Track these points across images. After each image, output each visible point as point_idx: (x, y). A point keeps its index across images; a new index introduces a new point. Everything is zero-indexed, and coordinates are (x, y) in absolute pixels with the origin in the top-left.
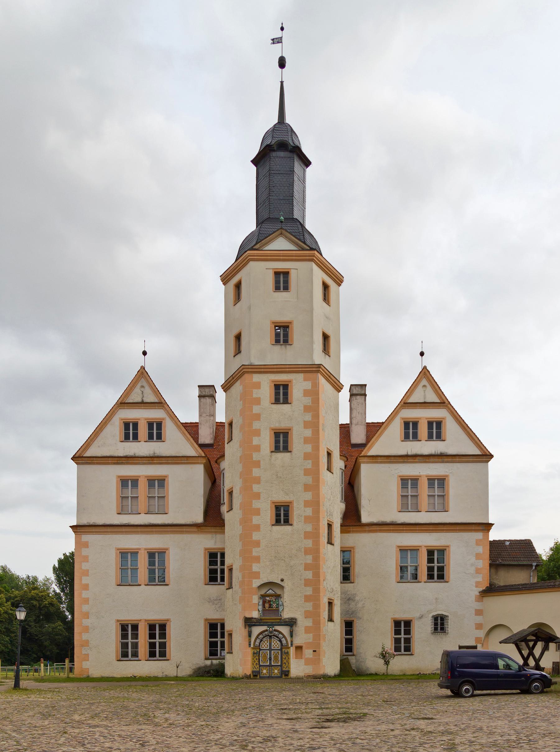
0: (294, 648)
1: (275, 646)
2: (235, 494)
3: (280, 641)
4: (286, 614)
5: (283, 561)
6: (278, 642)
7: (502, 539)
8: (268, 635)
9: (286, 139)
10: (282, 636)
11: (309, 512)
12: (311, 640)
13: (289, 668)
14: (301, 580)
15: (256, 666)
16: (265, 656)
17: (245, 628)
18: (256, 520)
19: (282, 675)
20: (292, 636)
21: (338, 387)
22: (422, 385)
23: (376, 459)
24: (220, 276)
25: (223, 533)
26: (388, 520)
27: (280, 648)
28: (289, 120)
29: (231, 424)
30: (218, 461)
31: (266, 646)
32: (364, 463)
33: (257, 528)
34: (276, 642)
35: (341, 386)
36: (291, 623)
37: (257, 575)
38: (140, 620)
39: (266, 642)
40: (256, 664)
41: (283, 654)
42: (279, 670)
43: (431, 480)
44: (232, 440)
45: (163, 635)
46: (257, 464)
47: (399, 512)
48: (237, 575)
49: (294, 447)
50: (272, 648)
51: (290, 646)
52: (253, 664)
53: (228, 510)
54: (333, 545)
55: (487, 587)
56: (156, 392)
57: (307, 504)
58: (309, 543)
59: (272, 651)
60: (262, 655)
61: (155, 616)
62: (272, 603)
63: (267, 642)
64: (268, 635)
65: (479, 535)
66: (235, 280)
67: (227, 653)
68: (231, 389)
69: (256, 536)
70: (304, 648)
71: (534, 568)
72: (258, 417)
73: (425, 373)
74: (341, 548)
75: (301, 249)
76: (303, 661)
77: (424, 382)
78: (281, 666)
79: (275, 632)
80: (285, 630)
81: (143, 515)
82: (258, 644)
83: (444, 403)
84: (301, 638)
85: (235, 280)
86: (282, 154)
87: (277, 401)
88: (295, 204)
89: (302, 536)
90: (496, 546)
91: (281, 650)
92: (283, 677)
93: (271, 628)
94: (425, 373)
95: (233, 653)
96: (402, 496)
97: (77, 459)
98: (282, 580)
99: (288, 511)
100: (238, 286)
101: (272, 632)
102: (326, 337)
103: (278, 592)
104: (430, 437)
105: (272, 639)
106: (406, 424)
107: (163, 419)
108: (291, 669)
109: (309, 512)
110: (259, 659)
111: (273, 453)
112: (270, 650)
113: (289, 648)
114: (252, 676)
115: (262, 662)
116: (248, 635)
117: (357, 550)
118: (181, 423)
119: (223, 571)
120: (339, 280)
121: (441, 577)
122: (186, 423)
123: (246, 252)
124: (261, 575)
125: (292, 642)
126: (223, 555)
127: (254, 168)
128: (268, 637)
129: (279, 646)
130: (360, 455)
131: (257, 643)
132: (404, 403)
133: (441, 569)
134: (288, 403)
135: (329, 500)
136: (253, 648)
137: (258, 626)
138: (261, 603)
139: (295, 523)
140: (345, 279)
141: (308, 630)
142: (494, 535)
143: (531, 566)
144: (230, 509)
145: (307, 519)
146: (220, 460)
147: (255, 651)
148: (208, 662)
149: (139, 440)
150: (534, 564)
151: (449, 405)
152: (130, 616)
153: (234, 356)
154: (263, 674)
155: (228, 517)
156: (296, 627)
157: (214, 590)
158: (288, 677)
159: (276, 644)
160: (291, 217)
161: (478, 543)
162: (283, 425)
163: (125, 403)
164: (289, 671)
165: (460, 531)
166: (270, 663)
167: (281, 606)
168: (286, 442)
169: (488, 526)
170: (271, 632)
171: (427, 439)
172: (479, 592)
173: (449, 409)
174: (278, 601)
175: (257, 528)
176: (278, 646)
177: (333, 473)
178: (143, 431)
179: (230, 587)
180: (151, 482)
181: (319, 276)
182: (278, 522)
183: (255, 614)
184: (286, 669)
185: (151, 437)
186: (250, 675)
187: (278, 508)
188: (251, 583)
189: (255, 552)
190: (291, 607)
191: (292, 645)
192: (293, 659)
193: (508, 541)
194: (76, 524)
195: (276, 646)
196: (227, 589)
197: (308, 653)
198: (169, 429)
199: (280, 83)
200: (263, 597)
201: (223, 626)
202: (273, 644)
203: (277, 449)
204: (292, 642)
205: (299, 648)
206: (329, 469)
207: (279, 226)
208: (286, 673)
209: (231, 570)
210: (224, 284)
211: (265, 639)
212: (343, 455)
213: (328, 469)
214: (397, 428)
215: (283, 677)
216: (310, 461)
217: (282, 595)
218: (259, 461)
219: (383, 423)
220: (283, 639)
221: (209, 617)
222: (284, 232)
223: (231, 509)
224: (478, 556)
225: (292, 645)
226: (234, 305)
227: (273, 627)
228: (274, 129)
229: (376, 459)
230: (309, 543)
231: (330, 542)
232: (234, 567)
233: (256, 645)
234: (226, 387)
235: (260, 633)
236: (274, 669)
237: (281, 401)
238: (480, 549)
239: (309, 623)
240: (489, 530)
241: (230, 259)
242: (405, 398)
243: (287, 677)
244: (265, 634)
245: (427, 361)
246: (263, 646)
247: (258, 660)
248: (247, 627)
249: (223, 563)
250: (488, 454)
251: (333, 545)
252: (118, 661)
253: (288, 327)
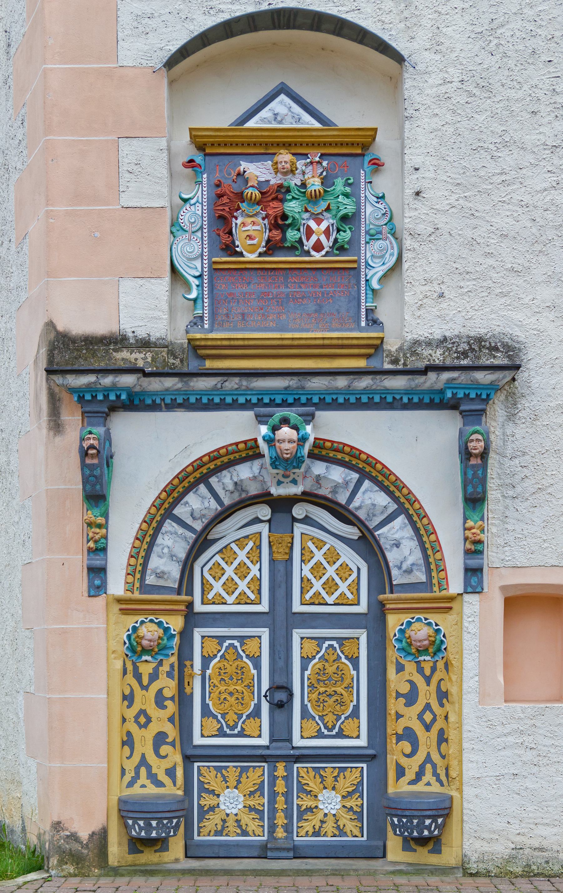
10: (382, 499)
27: (363, 608)
31: (242, 586)
42: (357, 789)
59: (297, 634)
79: (319, 468)
82: (175, 571)
108: (468, 791)
115: (212, 725)
128: (264, 512)
137: (172, 406)
156: (511, 417)
158: (434, 860)
176: (343, 587)
190: (472, 243)
192: (483, 697)
233: (150, 580)
235: (182, 476)
236: (313, 785)
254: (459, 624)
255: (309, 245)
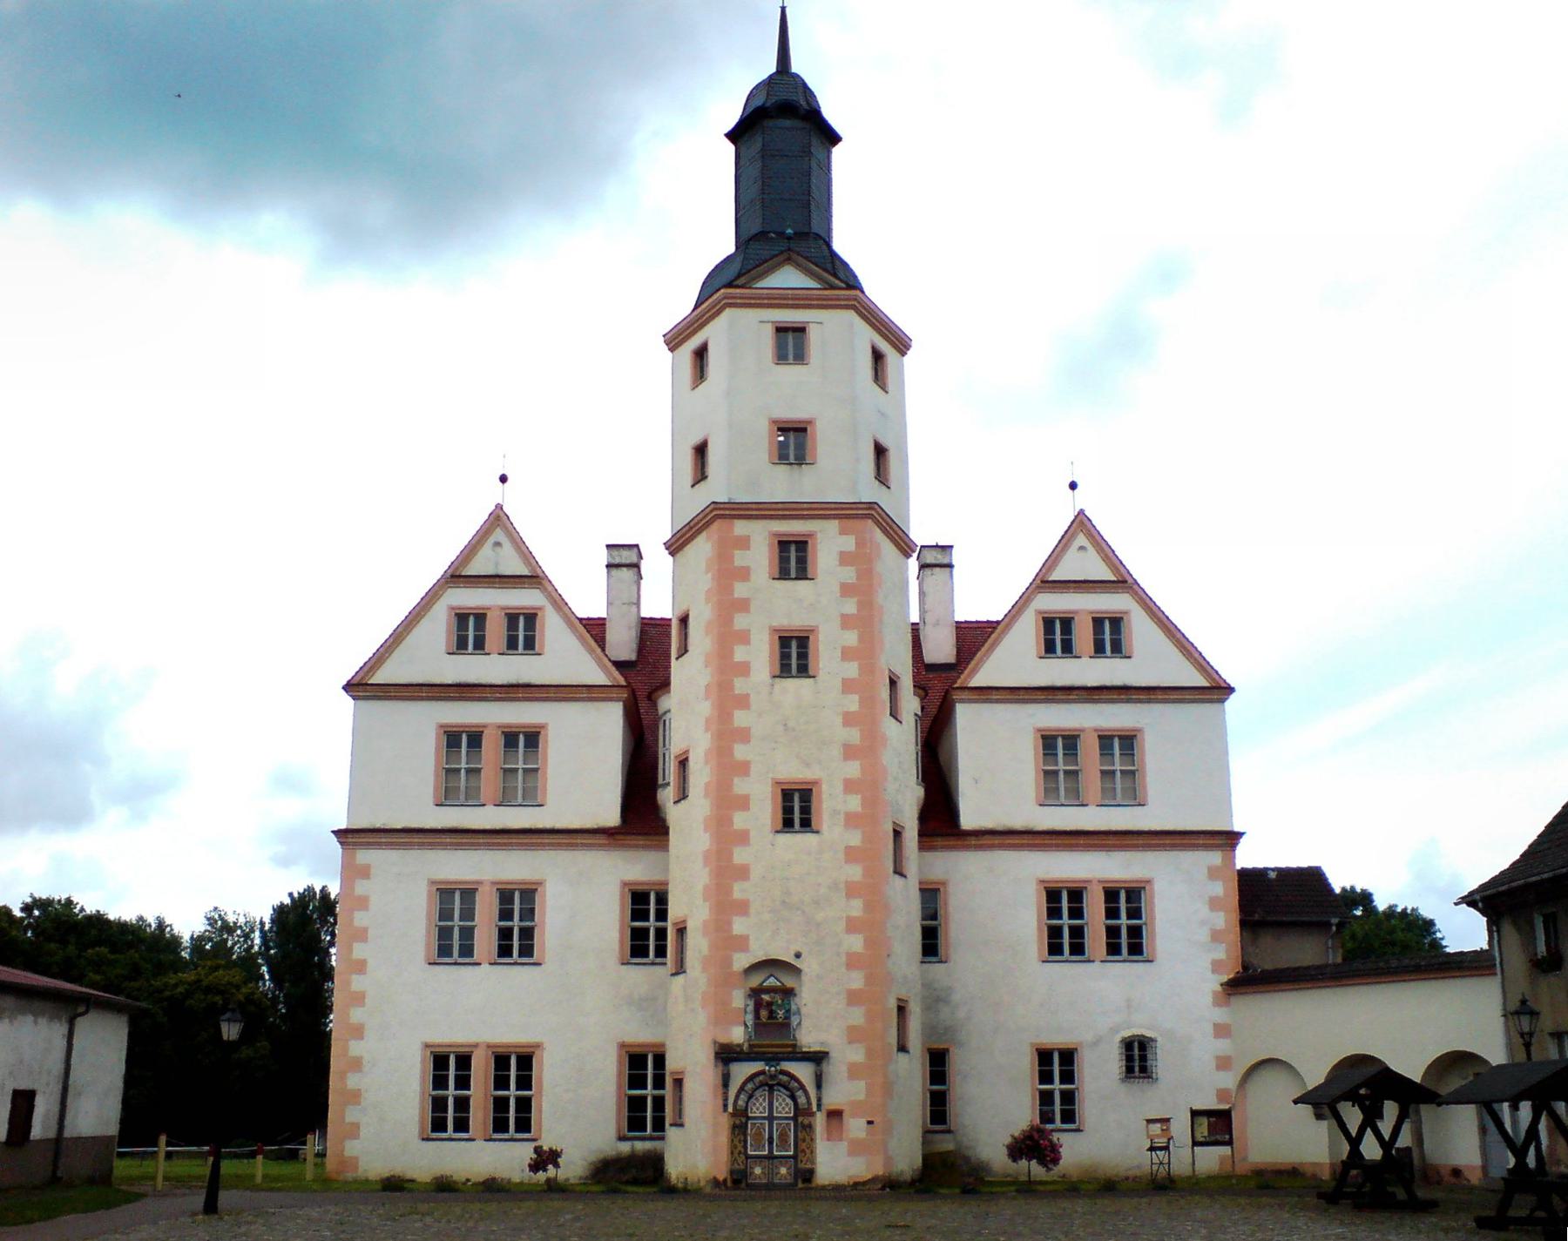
0: (825, 1114)
1: (780, 1109)
2: (693, 765)
3: (793, 1097)
4: (808, 1038)
5: (799, 912)
6: (788, 1100)
7: (1260, 865)
8: (767, 1084)
9: (795, 98)
10: (796, 1084)
11: (854, 803)
12: (862, 1097)
13: (813, 1163)
14: (838, 954)
15: (738, 1158)
16: (759, 1135)
17: (716, 1066)
18: (740, 820)
19: (796, 1178)
20: (819, 1086)
21: (905, 546)
22: (1077, 547)
23: (987, 694)
24: (664, 336)
25: (664, 846)
26: (1018, 823)
28: (796, 66)
29: (684, 620)
30: (653, 697)
32: (962, 701)
33: (743, 838)
34: (784, 1100)
35: (912, 546)
36: (818, 1058)
37: (742, 943)
38: (476, 1046)
39: (761, 1100)
40: (740, 1153)
41: (800, 1128)
43: (1105, 740)
44: (686, 651)
45: (525, 1082)
46: (743, 702)
47: (1041, 805)
48: (698, 945)
49: (821, 666)
50: (775, 1115)
51: (815, 1109)
52: (732, 1153)
53: (676, 799)
54: (905, 877)
55: (1238, 972)
56: (526, 555)
57: (850, 786)
58: (855, 872)
60: (752, 1130)
61: (511, 1035)
62: (774, 1008)
63: (764, 1100)
64: (767, 1084)
65: (1215, 858)
66: (695, 342)
67: (671, 1125)
68: (685, 549)
69: (740, 856)
70: (846, 1116)
71: (1334, 928)
72: (744, 605)
73: (1081, 523)
74: (920, 883)
75: (827, 286)
76: (843, 1146)
77: (1081, 540)
78: (795, 1157)
79: (781, 1076)
80: (803, 1072)
81: (490, 809)
83: (1125, 582)
84: (841, 1090)
85: (695, 342)
86: (788, 123)
87: (783, 574)
88: (813, 207)
89: (841, 855)
90: (1253, 884)
91: (795, 1118)
92: (800, 1185)
93: (772, 1066)
94: (1081, 523)
95: (687, 1125)
96: (1046, 773)
97: (356, 688)
98: (798, 956)
99: (810, 801)
100: (701, 354)
101: (775, 1076)
102: (880, 451)
103: (789, 982)
104: (1099, 649)
105: (775, 1093)
106: (1048, 623)
107: (540, 609)
108: (818, 1165)
109: (854, 803)
110: (746, 1142)
111: (777, 680)
112: (771, 1118)
113: (812, 1114)
114: (729, 1183)
115: (753, 1149)
116: (719, 1081)
117: (951, 889)
118: (578, 618)
119: (661, 934)
120: (902, 344)
121: (1136, 949)
122: (589, 619)
123: (718, 290)
124: (752, 942)
125: (819, 1100)
126: (662, 899)
127: (731, 148)
128: (767, 1088)
129: (790, 1109)
130: (955, 686)
131: (741, 1103)
132: (1042, 582)
133: (1136, 932)
134: (807, 579)
135: (896, 779)
136: (733, 1115)
138: (751, 1008)
139: (825, 828)
140: (913, 344)
141: (854, 1072)
142: (1248, 856)
143: (1328, 925)
144: (682, 796)
145: (851, 820)
146: (660, 693)
147: (738, 1122)
148: (625, 1147)
149: (486, 651)
150: (1335, 921)
151: (1135, 587)
152: (454, 1035)
153: (693, 486)
154: (753, 1177)
155: (674, 814)
157: (641, 976)
159: (784, 1106)
160: (806, 231)
161: (1213, 873)
162: (795, 620)
163: (460, 576)
164: (811, 1172)
165: (1173, 847)
166: (771, 1150)
167: (794, 1014)
168: (803, 656)
169: (1230, 839)
170: (773, 1077)
171: (1093, 654)
172: (1222, 985)
173: (1136, 593)
174: (789, 1004)
175: (743, 838)
177: (901, 722)
178: (496, 631)
179: (680, 969)
180: (510, 738)
181: (866, 336)
182: (788, 824)
183: (737, 1035)
184: (807, 1166)
185: (512, 644)
186: (725, 1180)
187: (787, 795)
188: (728, 962)
189: (739, 891)
191: (819, 1106)
193: (1273, 870)
194: (343, 826)
195: (783, 1108)
196: (673, 975)
197: (855, 1127)
198: (552, 629)
199: (780, 9)
200: (755, 993)
201: (660, 1060)
202: (776, 1104)
203: (784, 671)
204: (819, 1100)
205: (835, 1115)
206: (894, 714)
207: (784, 245)
208: (808, 1175)
209: (681, 931)
210: (672, 350)
211: (758, 1093)
212: (921, 688)
213: (891, 714)
214: (1027, 633)
215: (800, 1185)
216: (856, 697)
217: (797, 991)
218: (747, 696)
219: (998, 623)
220: (799, 1093)
221: (629, 1039)
222: (794, 256)
223: (683, 796)
224: (1214, 903)
225: (819, 1106)
226: (694, 388)
227: (778, 1064)
228: (770, 82)
229: (987, 694)
230: (855, 872)
231: (899, 871)
232: (690, 925)
234: (675, 546)
237: (793, 575)
238: (1218, 889)
239: (857, 1055)
240: (1233, 846)
241: (683, 304)
242: (1044, 571)
243: (806, 1185)
244: (760, 1081)
245: (1082, 499)
246: (754, 1109)
247: (742, 1144)
248: (721, 1067)
249: (662, 915)
250: (1223, 685)
251: (905, 877)
252: (423, 1139)
253: (804, 430)
254: (815, 1120)
255: (778, 1017)
